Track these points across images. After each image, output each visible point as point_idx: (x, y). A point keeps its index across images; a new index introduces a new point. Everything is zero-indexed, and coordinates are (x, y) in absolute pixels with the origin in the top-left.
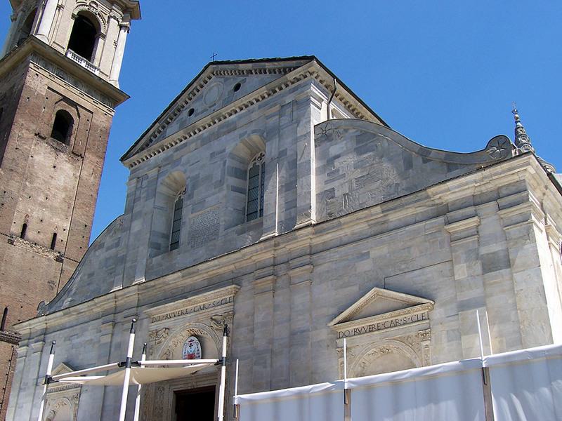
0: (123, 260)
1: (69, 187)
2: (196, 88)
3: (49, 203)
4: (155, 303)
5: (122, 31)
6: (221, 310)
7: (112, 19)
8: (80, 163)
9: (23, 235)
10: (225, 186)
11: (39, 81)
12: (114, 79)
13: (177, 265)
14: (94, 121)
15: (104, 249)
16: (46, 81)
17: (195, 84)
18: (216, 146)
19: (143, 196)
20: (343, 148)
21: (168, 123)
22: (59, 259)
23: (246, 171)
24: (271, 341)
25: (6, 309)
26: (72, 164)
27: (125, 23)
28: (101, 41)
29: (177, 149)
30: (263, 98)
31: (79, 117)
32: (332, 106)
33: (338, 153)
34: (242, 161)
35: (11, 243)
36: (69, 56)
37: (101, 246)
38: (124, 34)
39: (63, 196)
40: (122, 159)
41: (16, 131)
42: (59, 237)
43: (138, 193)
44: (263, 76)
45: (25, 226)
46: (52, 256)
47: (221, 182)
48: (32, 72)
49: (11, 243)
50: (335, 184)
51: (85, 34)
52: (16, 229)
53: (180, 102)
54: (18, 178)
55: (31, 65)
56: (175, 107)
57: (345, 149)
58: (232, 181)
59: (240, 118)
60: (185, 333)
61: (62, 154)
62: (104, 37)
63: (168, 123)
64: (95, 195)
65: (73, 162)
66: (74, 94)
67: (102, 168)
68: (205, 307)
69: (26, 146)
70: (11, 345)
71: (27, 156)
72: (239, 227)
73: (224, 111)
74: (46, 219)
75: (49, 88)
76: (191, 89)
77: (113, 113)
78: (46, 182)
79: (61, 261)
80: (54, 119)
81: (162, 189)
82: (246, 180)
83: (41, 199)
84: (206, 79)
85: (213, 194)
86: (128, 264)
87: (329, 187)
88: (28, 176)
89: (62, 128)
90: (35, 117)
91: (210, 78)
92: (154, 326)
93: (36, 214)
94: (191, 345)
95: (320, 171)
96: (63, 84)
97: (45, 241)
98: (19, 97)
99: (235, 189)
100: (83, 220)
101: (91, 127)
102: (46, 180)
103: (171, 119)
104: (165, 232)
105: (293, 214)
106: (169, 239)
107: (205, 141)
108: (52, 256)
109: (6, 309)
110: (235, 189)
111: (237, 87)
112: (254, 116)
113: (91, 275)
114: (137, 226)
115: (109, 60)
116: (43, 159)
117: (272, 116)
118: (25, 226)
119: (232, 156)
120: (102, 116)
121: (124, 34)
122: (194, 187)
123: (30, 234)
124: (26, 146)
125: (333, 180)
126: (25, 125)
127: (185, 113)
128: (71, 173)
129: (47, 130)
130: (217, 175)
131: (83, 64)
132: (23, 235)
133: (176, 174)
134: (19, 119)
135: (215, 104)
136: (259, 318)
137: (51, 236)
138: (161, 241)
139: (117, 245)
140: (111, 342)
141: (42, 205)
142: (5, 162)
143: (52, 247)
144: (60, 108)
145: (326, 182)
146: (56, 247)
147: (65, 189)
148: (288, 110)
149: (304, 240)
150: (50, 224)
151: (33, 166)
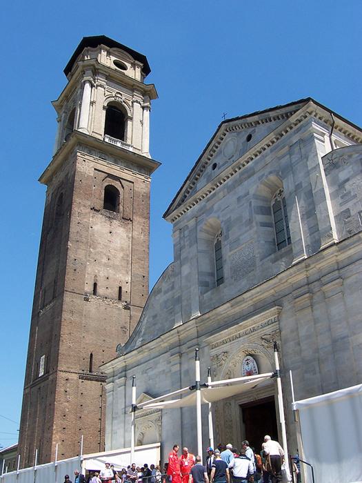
0: (179, 300)
1: (125, 246)
2: (214, 145)
3: (111, 263)
4: (212, 333)
5: (145, 111)
6: (268, 330)
7: (135, 104)
8: (130, 226)
9: (95, 292)
10: (254, 224)
11: (87, 166)
12: (145, 152)
13: (225, 297)
14: (137, 189)
15: (162, 293)
16: (92, 164)
17: (213, 142)
18: (240, 190)
19: (186, 244)
20: (349, 172)
21: (197, 179)
22: (127, 308)
23: (270, 208)
24: (317, 350)
25: (91, 354)
26: (124, 228)
27: (146, 104)
28: (129, 123)
29: (208, 200)
30: (273, 142)
31: (123, 188)
32: (334, 138)
33: (346, 178)
34: (265, 200)
35: (87, 300)
36: (107, 140)
37: (159, 291)
38: (147, 113)
39: (121, 255)
40: (165, 216)
41: (75, 209)
42: (124, 290)
43: (182, 242)
44: (269, 124)
45: (95, 285)
46: (120, 306)
47: (250, 221)
48: (80, 159)
49: (87, 300)
50: (349, 205)
51: (116, 120)
52: (89, 288)
53: (204, 160)
54: (83, 247)
55: (78, 154)
56: (200, 165)
57: (352, 172)
58: (260, 218)
59: (256, 163)
60: (241, 354)
61: (115, 221)
62: (131, 119)
63: (197, 179)
64: (147, 250)
65: (124, 226)
66: (116, 170)
68: (254, 330)
69: (85, 220)
70: (100, 383)
71: (88, 228)
72: (273, 256)
73: (242, 160)
74: (111, 276)
75: (95, 169)
76: (210, 147)
77: (149, 180)
78: (106, 246)
79: (129, 309)
80: (103, 193)
81: (202, 235)
82: (271, 215)
83: (104, 260)
84: (222, 136)
85: (246, 232)
86: (184, 303)
87: (344, 208)
88: (91, 244)
89: (111, 199)
90: (88, 195)
91: (225, 135)
92: (214, 352)
93: (102, 274)
94: (248, 364)
95: (333, 196)
96: (105, 164)
97: (115, 296)
98: (73, 181)
99: (264, 225)
100: (140, 272)
101: (134, 196)
102: (106, 244)
103: (199, 175)
104: (210, 271)
105: (317, 237)
106: (214, 276)
107: (230, 189)
108: (120, 306)
109: (91, 354)
110: (264, 225)
111: (249, 138)
112: (268, 159)
113: (155, 317)
114: (186, 270)
115: (139, 137)
116: (100, 228)
117: (283, 156)
118: (95, 285)
119: (256, 197)
120: (141, 184)
121: (147, 113)
122: (228, 230)
123: (100, 291)
124: (85, 220)
125: (347, 202)
126: (82, 203)
127: (210, 168)
128: (125, 235)
129: (100, 203)
130: (246, 215)
131: (119, 145)
132: (95, 292)
133: (212, 220)
134: (77, 199)
135: (233, 156)
136: (303, 332)
138: (208, 279)
139: (173, 288)
140: (180, 370)
141: (106, 265)
142: (71, 235)
143: (120, 298)
144: (106, 184)
145: (341, 205)
146: (123, 298)
147: (122, 249)
148: (296, 149)
149: (331, 258)
150: (115, 280)
151: (94, 235)
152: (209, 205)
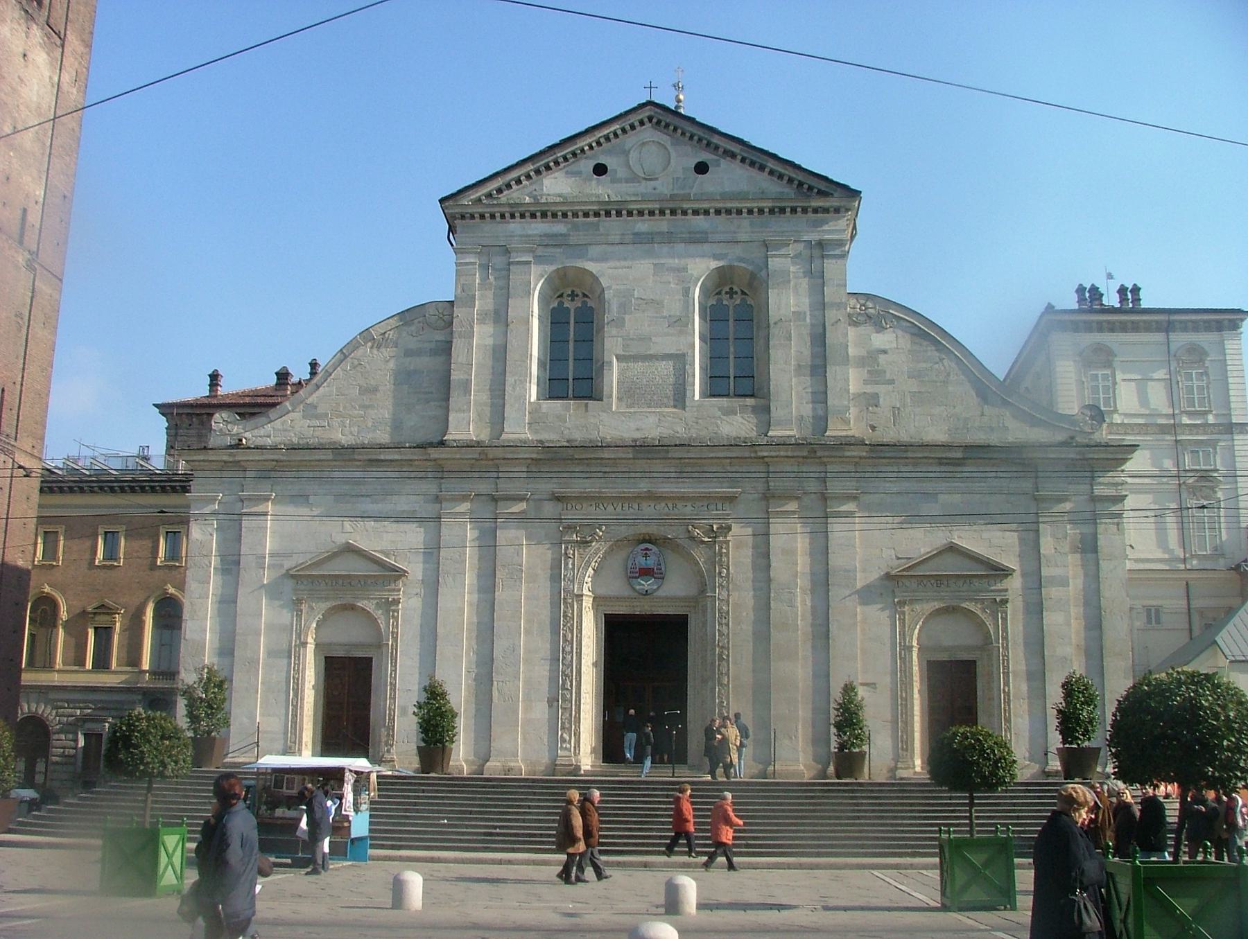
22: (30, 266)
29: (576, 227)
40: (442, 201)
50: (881, 389)
53: (583, 143)
64: (77, 129)
65: (48, 47)
67: (88, 69)
84: (637, 124)
87: (870, 389)
91: (642, 123)
108: (21, 259)
111: (701, 168)
122: (624, 307)
130: (673, 307)
135: (656, 179)
137: (20, 212)
145: (866, 382)
152: (573, 240)
